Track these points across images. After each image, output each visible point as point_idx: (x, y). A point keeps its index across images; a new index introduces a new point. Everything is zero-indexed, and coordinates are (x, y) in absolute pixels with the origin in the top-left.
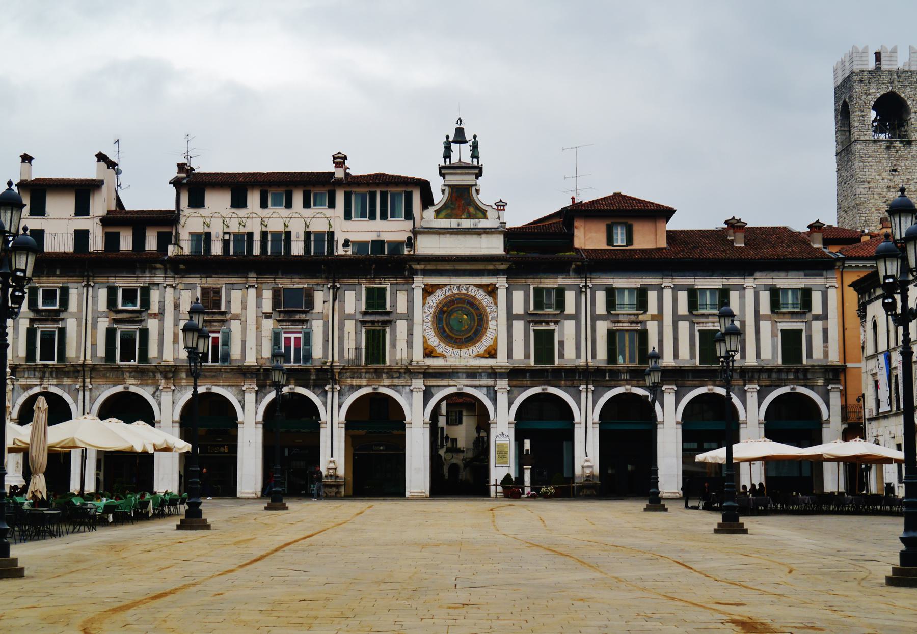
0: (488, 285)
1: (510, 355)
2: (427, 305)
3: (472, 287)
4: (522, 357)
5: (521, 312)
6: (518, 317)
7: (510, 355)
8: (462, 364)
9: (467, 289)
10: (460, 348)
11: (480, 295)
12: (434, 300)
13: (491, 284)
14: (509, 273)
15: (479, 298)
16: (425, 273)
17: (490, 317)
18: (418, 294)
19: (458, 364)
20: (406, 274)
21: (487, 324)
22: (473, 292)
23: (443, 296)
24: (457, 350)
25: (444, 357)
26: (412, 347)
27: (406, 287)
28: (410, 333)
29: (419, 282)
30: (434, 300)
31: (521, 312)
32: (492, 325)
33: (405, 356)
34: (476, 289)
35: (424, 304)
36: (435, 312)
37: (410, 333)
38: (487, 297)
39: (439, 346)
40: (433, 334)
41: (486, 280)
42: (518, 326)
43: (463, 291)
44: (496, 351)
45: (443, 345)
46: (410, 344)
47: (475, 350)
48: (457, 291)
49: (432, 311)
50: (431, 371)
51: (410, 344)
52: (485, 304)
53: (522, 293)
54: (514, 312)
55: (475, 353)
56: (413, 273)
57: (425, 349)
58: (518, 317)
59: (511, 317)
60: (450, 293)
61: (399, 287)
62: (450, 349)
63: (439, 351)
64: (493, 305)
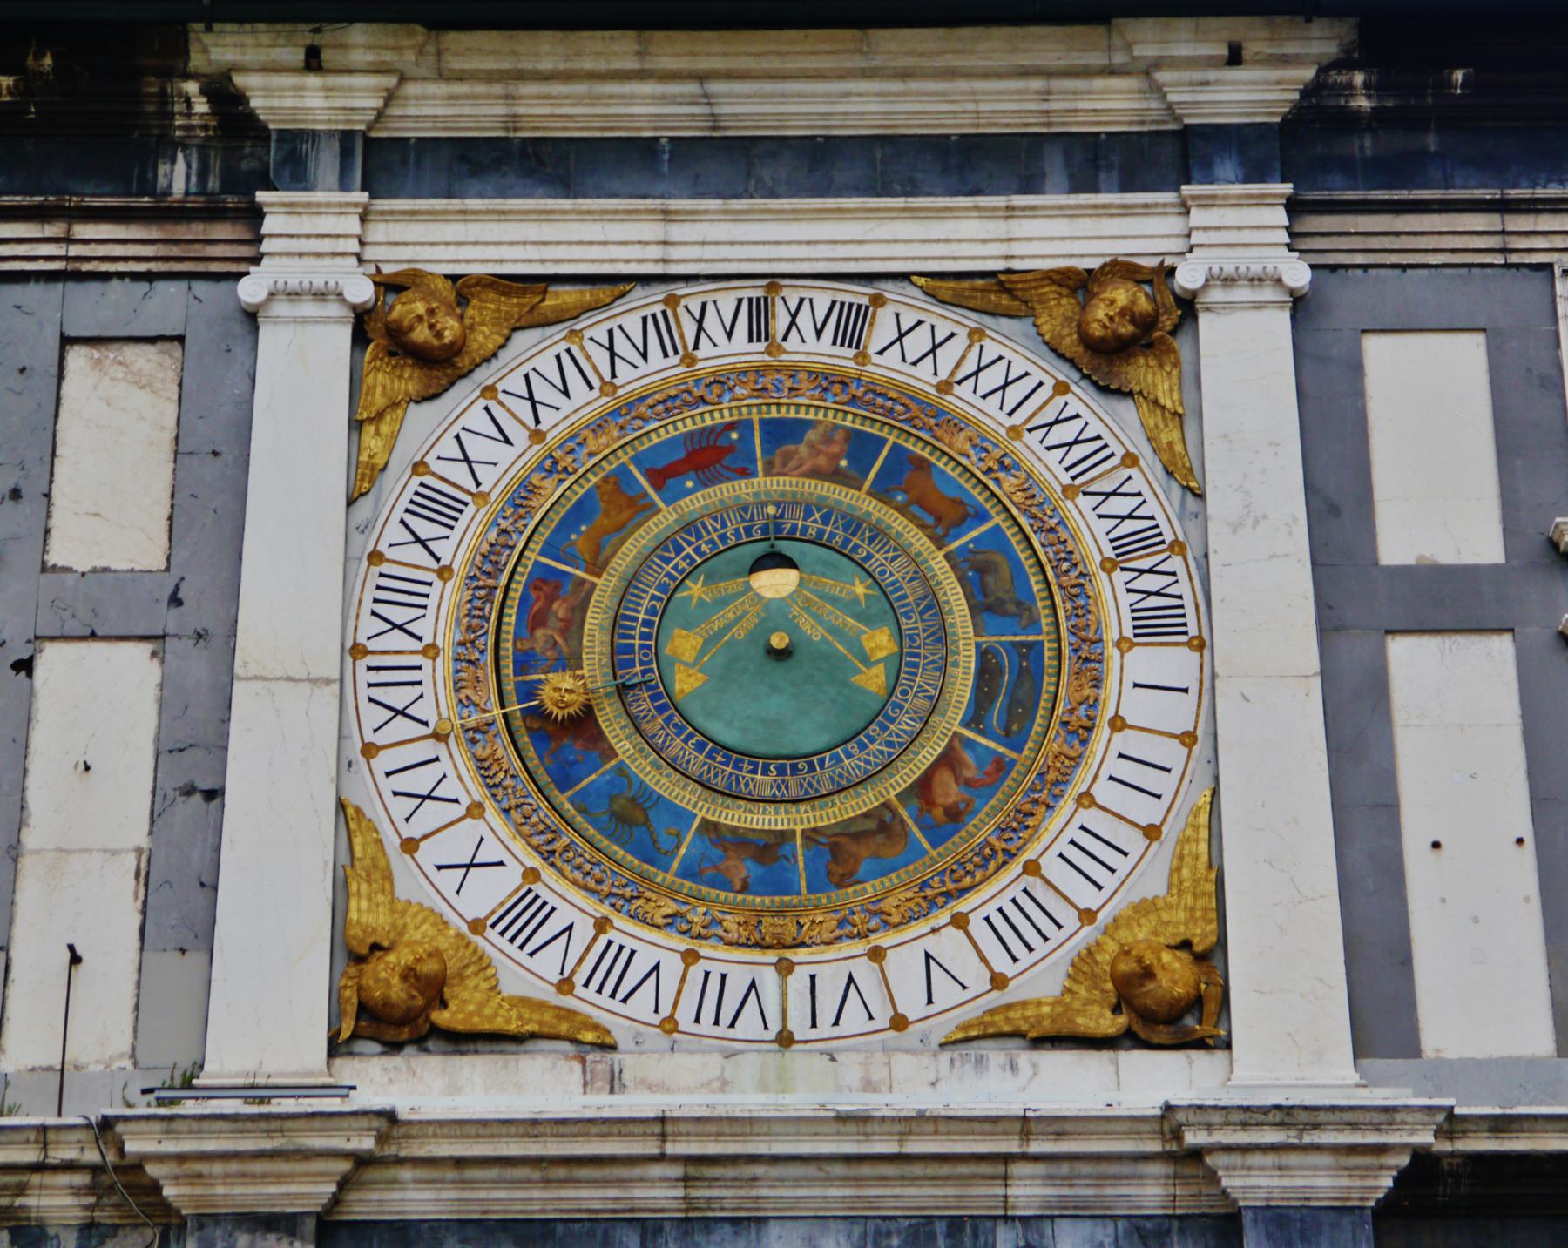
0: (1080, 284)
1: (1382, 1012)
2: (398, 488)
3: (904, 305)
4: (1538, 1038)
5: (1478, 541)
6: (1445, 602)
7: (1382, 1012)
8: (800, 1100)
9: (851, 327)
10: (780, 945)
11: (1004, 386)
12: (483, 438)
13: (1120, 270)
14: (1302, 154)
15: (992, 416)
16: (385, 163)
17: (1114, 603)
18: (303, 373)
19: (745, 1100)
20: (178, 177)
21: (1090, 667)
22: (913, 349)
23: (584, 401)
24: (741, 967)
25: (592, 1045)
26: (201, 937)
27: (167, 305)
28: (192, 781)
29: (317, 243)
30: (483, 438)
31: (1478, 541)
32: (1142, 684)
33: (104, 1034)
34: (945, 320)
35: (362, 482)
36: (489, 560)
37: (192, 781)
38: (1081, 400)
39: (523, 917)
40: (463, 783)
41: (1058, 232)
42: (1455, 699)
43: (810, 347)
44: (1210, 957)
45: (571, 906)
46: (180, 905)
47: (941, 961)
48: (741, 349)
49: (460, 544)
50: (413, 1199)
51: (180, 905)
52: (1051, 469)
53: (1470, 351)
54: (1401, 540)
55: (963, 995)
56: (254, 160)
57: (355, 954)
58: (1445, 602)
59: (1363, 602)
60: (660, 367)
61: (92, 307)
62: (653, 948)
63: (523, 975)
64: (1147, 478)
